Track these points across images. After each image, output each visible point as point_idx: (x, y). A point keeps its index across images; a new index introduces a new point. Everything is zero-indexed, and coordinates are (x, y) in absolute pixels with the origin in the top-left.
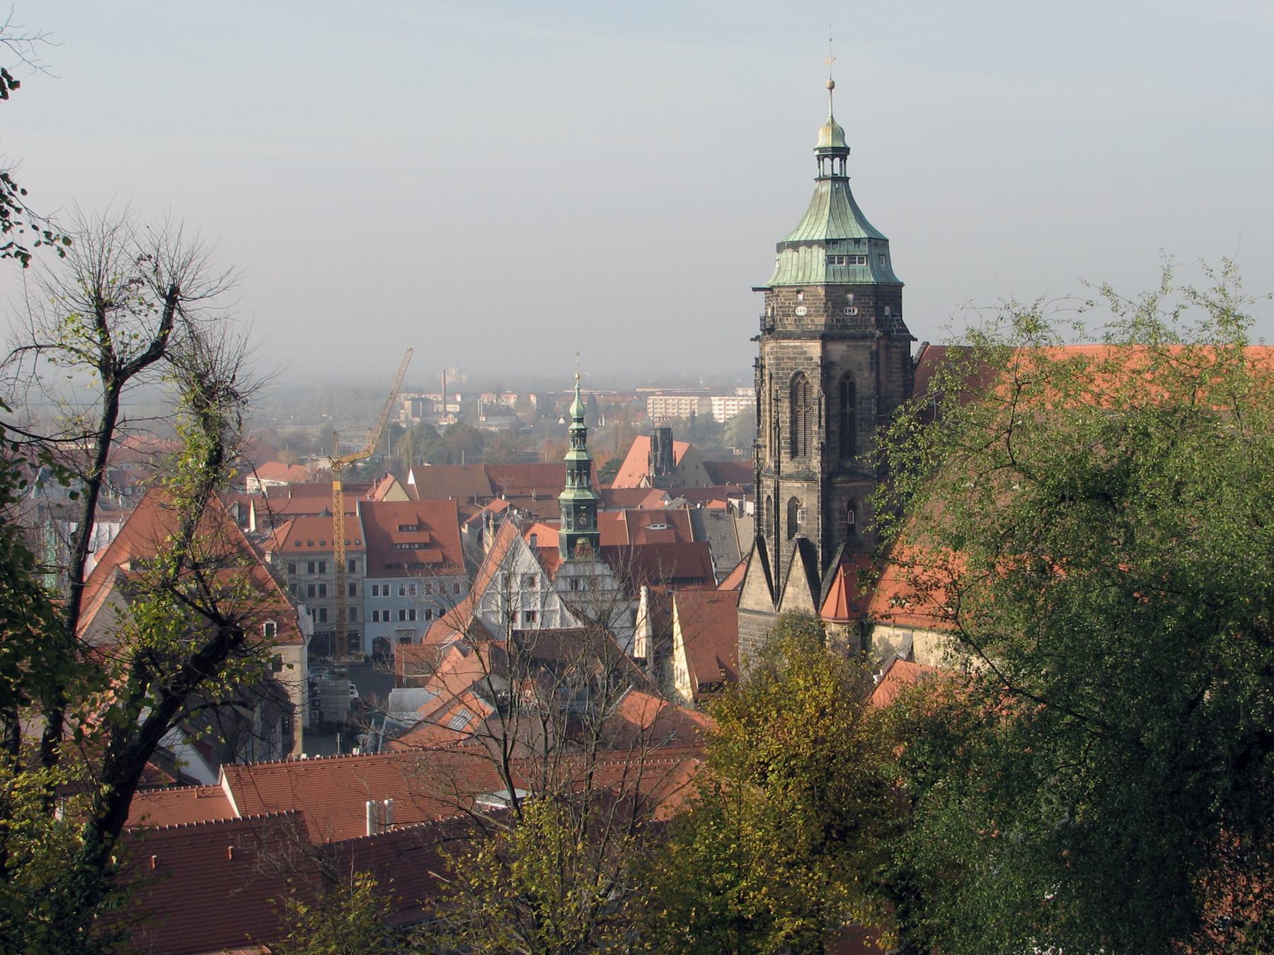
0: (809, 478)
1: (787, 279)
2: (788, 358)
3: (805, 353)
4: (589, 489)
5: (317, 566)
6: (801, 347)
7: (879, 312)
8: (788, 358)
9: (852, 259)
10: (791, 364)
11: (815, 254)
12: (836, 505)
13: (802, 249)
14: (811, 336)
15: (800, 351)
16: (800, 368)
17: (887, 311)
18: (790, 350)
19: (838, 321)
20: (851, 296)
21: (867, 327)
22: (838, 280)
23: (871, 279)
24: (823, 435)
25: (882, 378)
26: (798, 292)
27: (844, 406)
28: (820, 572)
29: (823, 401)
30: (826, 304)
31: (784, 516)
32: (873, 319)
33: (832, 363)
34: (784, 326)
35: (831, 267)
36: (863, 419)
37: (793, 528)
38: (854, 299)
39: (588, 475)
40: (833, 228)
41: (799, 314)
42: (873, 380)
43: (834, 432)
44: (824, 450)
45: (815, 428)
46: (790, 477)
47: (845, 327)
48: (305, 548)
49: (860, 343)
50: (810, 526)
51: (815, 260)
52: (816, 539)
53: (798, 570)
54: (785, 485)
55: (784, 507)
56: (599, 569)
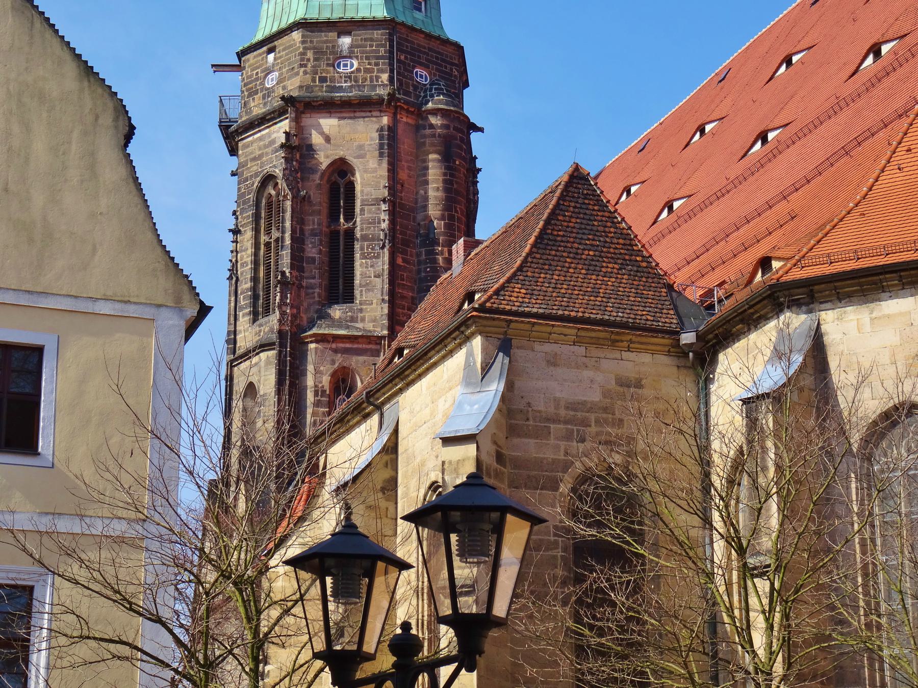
2: (254, 159)
6: (269, 134)
8: (254, 159)
15: (267, 141)
18: (255, 145)
20: (346, 41)
21: (374, 87)
25: (403, 175)
32: (385, 77)
36: (365, 238)
38: (352, 46)
42: (383, 170)
43: (313, 259)
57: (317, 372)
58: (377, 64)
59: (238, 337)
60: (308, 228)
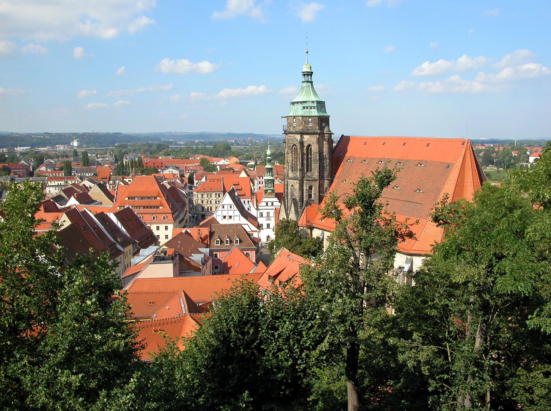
1: (291, 114)
3: (296, 138)
4: (272, 176)
9: (311, 108)
10: (292, 142)
11: (299, 106)
13: (296, 104)
14: (296, 133)
16: (294, 143)
19: (306, 128)
20: (310, 120)
21: (315, 130)
26: (294, 118)
31: (289, 191)
32: (318, 127)
34: (290, 129)
37: (292, 195)
39: (272, 172)
45: (298, 163)
46: (291, 179)
47: (308, 130)
50: (297, 195)
51: (299, 108)
52: (298, 199)
53: (293, 209)
54: (290, 181)
56: (276, 199)
57: (306, 186)
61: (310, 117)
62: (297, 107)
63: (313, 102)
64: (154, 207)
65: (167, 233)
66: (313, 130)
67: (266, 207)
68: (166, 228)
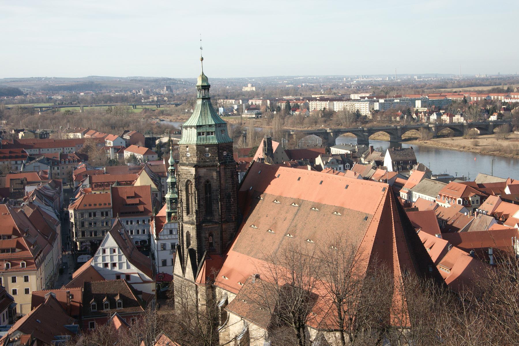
0: (192, 224)
2: (185, 174)
3: (190, 172)
5: (92, 214)
6: (189, 170)
7: (220, 155)
8: (185, 174)
9: (208, 133)
12: (203, 235)
13: (188, 129)
15: (188, 171)
16: (189, 178)
17: (225, 153)
18: (185, 170)
19: (202, 159)
20: (207, 149)
21: (214, 161)
22: (202, 143)
23: (215, 142)
24: (197, 207)
25: (222, 182)
26: (187, 147)
27: (206, 194)
28: (197, 263)
29: (196, 192)
30: (197, 152)
31: (185, 239)
32: (217, 158)
33: (200, 177)
35: (199, 137)
38: (209, 150)
40: (200, 120)
41: (188, 156)
44: (197, 212)
46: (186, 223)
48: (88, 207)
49: (211, 168)
50: (194, 244)
55: (185, 235)
58: (215, 155)
59: (184, 217)
60: (201, 197)
61: (206, 146)
62: (191, 132)
63: (210, 126)
64: (8, 251)
65: (26, 285)
66: (211, 161)
67: (170, 237)
68: (26, 279)
